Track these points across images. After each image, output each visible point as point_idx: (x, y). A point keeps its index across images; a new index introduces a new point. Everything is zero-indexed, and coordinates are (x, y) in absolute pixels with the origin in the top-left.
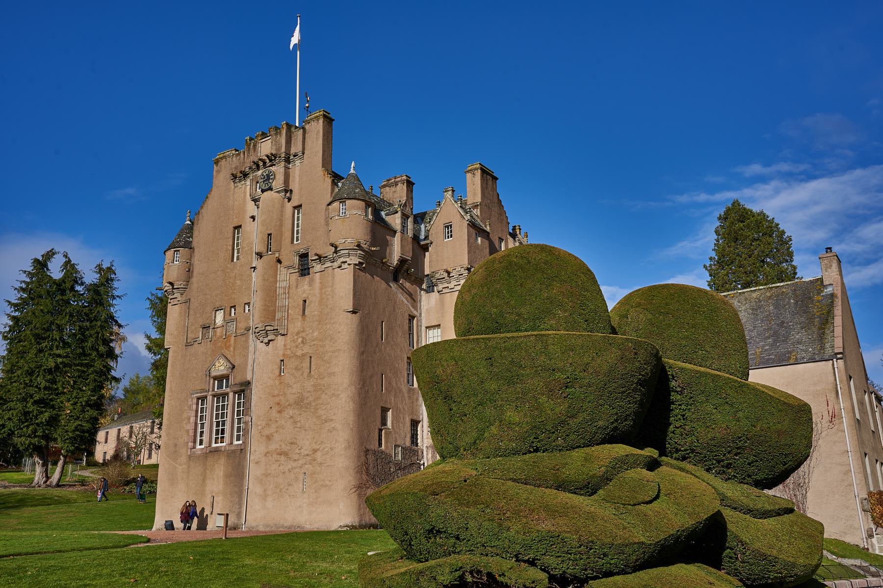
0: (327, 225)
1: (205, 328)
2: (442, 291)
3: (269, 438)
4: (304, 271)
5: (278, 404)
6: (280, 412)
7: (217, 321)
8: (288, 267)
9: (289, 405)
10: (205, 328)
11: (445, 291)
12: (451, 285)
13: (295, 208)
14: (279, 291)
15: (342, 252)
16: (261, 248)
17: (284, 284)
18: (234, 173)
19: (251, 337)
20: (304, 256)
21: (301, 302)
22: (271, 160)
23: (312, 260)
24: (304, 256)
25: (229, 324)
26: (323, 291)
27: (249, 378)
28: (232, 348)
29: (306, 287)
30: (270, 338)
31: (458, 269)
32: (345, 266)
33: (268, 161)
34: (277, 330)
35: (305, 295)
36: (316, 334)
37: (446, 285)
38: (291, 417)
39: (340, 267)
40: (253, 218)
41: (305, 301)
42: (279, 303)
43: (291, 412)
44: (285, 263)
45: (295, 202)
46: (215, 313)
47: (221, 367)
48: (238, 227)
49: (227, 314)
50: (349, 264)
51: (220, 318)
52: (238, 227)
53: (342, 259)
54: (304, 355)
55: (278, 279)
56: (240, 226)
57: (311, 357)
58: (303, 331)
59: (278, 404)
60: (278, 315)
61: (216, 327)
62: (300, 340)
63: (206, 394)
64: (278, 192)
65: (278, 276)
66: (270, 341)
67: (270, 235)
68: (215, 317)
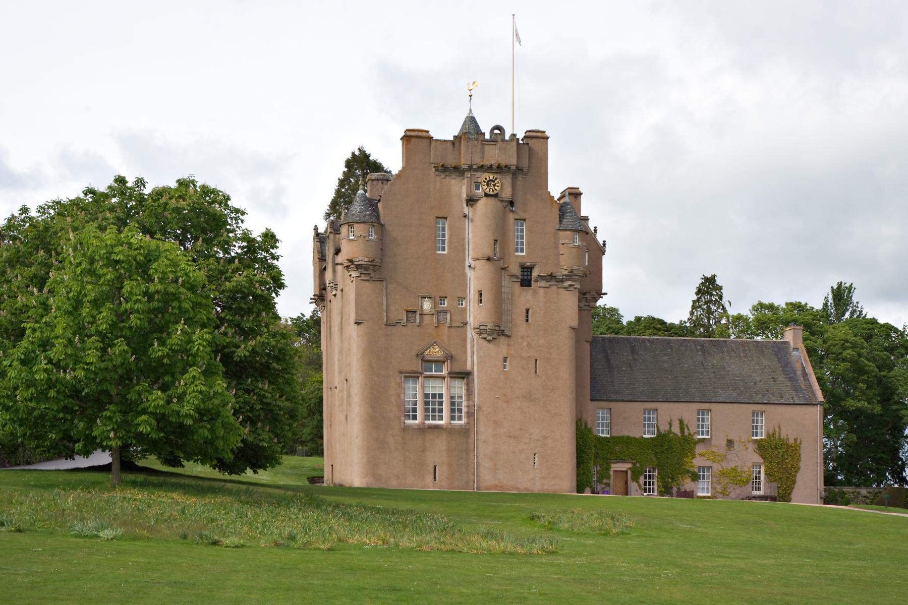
3: (497, 424)
5: (505, 395)
6: (507, 402)
9: (516, 397)
20: (527, 269)
21: (525, 311)
24: (527, 269)
26: (548, 305)
27: (469, 368)
28: (445, 338)
29: (529, 297)
32: (572, 288)
34: (503, 331)
36: (541, 342)
38: (520, 408)
41: (527, 311)
43: (519, 404)
47: (436, 352)
50: (575, 288)
51: (427, 305)
53: (570, 283)
54: (529, 357)
55: (503, 284)
57: (536, 360)
58: (528, 336)
59: (505, 395)
60: (504, 318)
62: (525, 344)
63: (419, 375)
64: (502, 201)
65: (503, 282)
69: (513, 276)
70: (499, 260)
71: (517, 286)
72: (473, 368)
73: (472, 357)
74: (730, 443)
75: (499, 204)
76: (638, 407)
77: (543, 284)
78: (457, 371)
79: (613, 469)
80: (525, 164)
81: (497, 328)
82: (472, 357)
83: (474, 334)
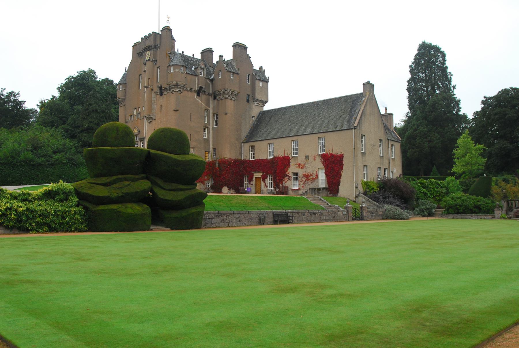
0: (167, 75)
1: (131, 116)
2: (218, 99)
4: (161, 94)
7: (135, 113)
8: (156, 92)
10: (131, 116)
11: (219, 99)
12: (221, 97)
13: (158, 68)
14: (153, 102)
15: (172, 87)
16: (146, 85)
17: (154, 99)
18: (138, 52)
19: (145, 120)
21: (160, 107)
22: (149, 48)
23: (163, 90)
24: (160, 88)
25: (138, 115)
29: (161, 100)
30: (150, 120)
31: (223, 90)
32: (173, 92)
33: (148, 48)
35: (161, 104)
37: (219, 97)
39: (172, 92)
40: (145, 71)
41: (161, 106)
42: (153, 107)
44: (155, 91)
45: (158, 66)
46: (134, 110)
48: (140, 75)
49: (138, 111)
50: (175, 92)
52: (140, 75)
56: (141, 75)
60: (153, 111)
61: (134, 115)
62: (160, 121)
64: (152, 61)
66: (151, 121)
67: (149, 79)
68: (134, 111)
69: (156, 92)
70: (150, 87)
71: (158, 96)
72: (145, 136)
73: (145, 131)
74: (307, 157)
75: (151, 62)
76: (265, 143)
77: (165, 93)
78: (141, 138)
79: (254, 177)
80: (158, 43)
81: (149, 117)
82: (145, 131)
83: (146, 121)
